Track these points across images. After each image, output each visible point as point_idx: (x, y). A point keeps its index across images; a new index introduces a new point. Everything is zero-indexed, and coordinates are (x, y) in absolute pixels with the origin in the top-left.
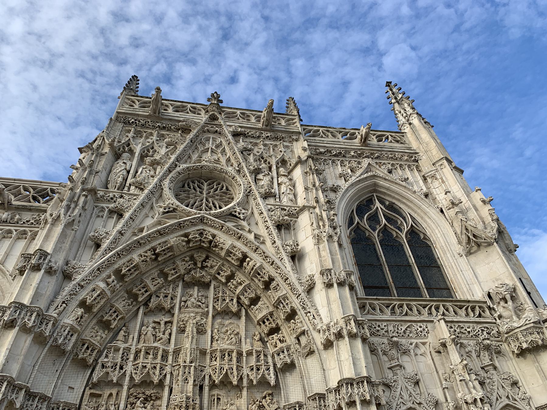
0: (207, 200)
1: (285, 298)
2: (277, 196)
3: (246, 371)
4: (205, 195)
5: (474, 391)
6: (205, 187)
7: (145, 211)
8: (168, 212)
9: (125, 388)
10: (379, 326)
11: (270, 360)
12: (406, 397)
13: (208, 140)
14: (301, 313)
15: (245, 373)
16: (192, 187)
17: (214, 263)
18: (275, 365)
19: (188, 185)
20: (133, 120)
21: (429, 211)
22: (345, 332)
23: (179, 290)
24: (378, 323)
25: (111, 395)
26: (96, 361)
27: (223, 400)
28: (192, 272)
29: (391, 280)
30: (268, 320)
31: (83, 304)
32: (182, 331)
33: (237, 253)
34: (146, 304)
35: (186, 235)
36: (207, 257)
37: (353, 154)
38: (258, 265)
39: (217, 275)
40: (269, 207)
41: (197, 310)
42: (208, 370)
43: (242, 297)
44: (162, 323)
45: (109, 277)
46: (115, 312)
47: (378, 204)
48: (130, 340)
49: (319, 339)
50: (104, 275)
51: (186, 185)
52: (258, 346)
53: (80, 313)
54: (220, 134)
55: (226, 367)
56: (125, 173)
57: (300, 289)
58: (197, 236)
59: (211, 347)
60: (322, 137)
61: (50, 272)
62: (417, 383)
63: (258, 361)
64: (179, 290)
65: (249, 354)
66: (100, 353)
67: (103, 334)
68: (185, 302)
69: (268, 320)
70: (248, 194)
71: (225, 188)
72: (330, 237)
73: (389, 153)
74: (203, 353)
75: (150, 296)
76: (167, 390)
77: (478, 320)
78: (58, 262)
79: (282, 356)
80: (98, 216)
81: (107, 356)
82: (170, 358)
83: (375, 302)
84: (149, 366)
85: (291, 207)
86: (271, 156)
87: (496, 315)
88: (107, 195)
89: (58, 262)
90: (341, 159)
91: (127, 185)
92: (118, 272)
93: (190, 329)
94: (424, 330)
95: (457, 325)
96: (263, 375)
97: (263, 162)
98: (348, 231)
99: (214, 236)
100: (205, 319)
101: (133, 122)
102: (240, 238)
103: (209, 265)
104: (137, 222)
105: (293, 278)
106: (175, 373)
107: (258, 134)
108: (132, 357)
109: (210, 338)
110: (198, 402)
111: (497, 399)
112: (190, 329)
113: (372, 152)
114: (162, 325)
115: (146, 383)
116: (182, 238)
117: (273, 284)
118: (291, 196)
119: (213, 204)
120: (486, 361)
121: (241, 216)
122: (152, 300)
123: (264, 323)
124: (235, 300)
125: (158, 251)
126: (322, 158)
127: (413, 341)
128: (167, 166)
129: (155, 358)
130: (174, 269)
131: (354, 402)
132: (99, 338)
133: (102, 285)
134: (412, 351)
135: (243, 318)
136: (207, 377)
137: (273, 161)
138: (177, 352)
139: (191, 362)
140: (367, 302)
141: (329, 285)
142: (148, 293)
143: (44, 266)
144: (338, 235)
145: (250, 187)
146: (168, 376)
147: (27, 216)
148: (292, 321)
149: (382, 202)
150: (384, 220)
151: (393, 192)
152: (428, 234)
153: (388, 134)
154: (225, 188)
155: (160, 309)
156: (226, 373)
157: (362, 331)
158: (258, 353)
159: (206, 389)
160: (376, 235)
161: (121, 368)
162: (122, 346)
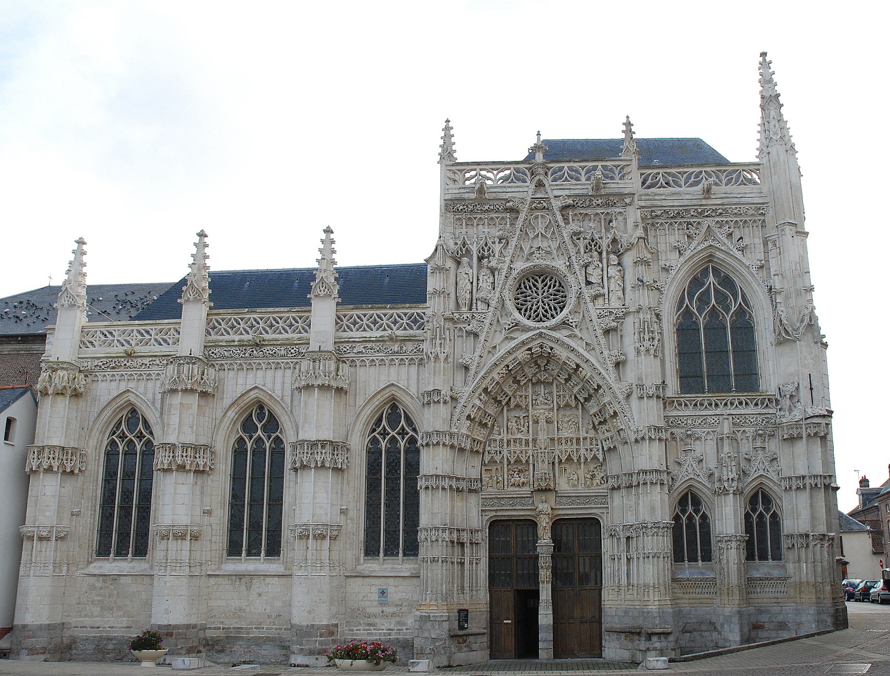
0: (543, 302)
1: (610, 403)
2: (606, 297)
3: (582, 452)
4: (540, 297)
5: (730, 473)
6: (540, 286)
7: (494, 327)
8: (513, 327)
9: (505, 466)
10: (681, 420)
11: (599, 443)
12: (690, 470)
13: (537, 217)
14: (620, 415)
15: (582, 453)
16: (528, 288)
17: (554, 368)
18: (603, 448)
19: (524, 283)
20: (461, 207)
21: (758, 289)
22: (647, 437)
23: (530, 390)
24: (681, 418)
25: (497, 469)
26: (484, 449)
27: (568, 471)
28: (538, 375)
29: (705, 370)
30: (598, 414)
31: (469, 417)
32: (536, 422)
33: (571, 364)
34: (508, 404)
35: (530, 349)
36: (548, 362)
37: (692, 214)
38: (589, 375)
39: (557, 377)
40: (598, 311)
41: (545, 407)
42: (557, 452)
43: (578, 396)
44: (521, 417)
45: (480, 395)
46: (488, 416)
47: (711, 278)
48: (502, 433)
49: (633, 437)
50: (477, 394)
51: (522, 286)
52: (592, 434)
53: (469, 425)
54: (548, 209)
55: (569, 450)
56: (469, 285)
57: (621, 397)
58: (538, 349)
59: (558, 435)
60: (662, 186)
61: (445, 402)
62: (702, 461)
63: (591, 444)
64: (530, 390)
65: (585, 439)
66: (485, 443)
67: (485, 432)
68: (536, 400)
69: (598, 414)
70: (579, 296)
71: (557, 284)
72: (648, 351)
73: (734, 207)
74: (552, 440)
75: (510, 399)
76: (531, 466)
77: (766, 411)
78: (445, 391)
79: (607, 443)
80: (459, 336)
81: (489, 446)
82: (530, 444)
83: (681, 399)
84: (518, 452)
85: (618, 309)
86: (601, 238)
87: (779, 407)
88: (462, 317)
89: (445, 391)
90: (680, 221)
91: (474, 301)
92: (486, 390)
93: (542, 422)
94: (715, 421)
95: (743, 417)
96: (595, 455)
97: (593, 246)
98: (676, 318)
99: (552, 349)
100: (552, 413)
101: (461, 210)
102: (573, 350)
103: (550, 369)
104: (489, 340)
105: (615, 386)
106: (535, 455)
107: (587, 203)
108: (505, 445)
109: (556, 429)
110: (552, 475)
111: (756, 471)
112: (542, 422)
113: (714, 207)
114: (522, 421)
115: (518, 461)
116: (528, 352)
117: (601, 391)
118: (620, 293)
119: (549, 305)
120: (759, 444)
121: (574, 325)
122: (512, 402)
123: (595, 416)
124: (573, 397)
125: (510, 369)
126: (658, 221)
127: (705, 430)
128: (504, 274)
129: (521, 445)
130: (524, 376)
131: (647, 483)
132: (482, 435)
133: (478, 402)
134: (703, 438)
135: (581, 411)
136: (557, 457)
137: (605, 243)
138: (535, 440)
139: (545, 449)
140: (675, 399)
141: (642, 398)
142: (508, 398)
143: (441, 400)
144: (655, 347)
145: (580, 289)
146: (531, 457)
147: (410, 346)
148: (615, 420)
149: (716, 272)
150: (713, 300)
151: (728, 264)
152: (753, 315)
153: (741, 168)
154: (557, 284)
155: (518, 406)
156: (569, 454)
157: (660, 434)
158: (591, 439)
159: (557, 465)
160: (701, 320)
161: (500, 453)
162: (498, 438)
